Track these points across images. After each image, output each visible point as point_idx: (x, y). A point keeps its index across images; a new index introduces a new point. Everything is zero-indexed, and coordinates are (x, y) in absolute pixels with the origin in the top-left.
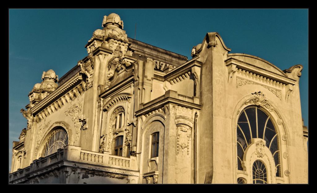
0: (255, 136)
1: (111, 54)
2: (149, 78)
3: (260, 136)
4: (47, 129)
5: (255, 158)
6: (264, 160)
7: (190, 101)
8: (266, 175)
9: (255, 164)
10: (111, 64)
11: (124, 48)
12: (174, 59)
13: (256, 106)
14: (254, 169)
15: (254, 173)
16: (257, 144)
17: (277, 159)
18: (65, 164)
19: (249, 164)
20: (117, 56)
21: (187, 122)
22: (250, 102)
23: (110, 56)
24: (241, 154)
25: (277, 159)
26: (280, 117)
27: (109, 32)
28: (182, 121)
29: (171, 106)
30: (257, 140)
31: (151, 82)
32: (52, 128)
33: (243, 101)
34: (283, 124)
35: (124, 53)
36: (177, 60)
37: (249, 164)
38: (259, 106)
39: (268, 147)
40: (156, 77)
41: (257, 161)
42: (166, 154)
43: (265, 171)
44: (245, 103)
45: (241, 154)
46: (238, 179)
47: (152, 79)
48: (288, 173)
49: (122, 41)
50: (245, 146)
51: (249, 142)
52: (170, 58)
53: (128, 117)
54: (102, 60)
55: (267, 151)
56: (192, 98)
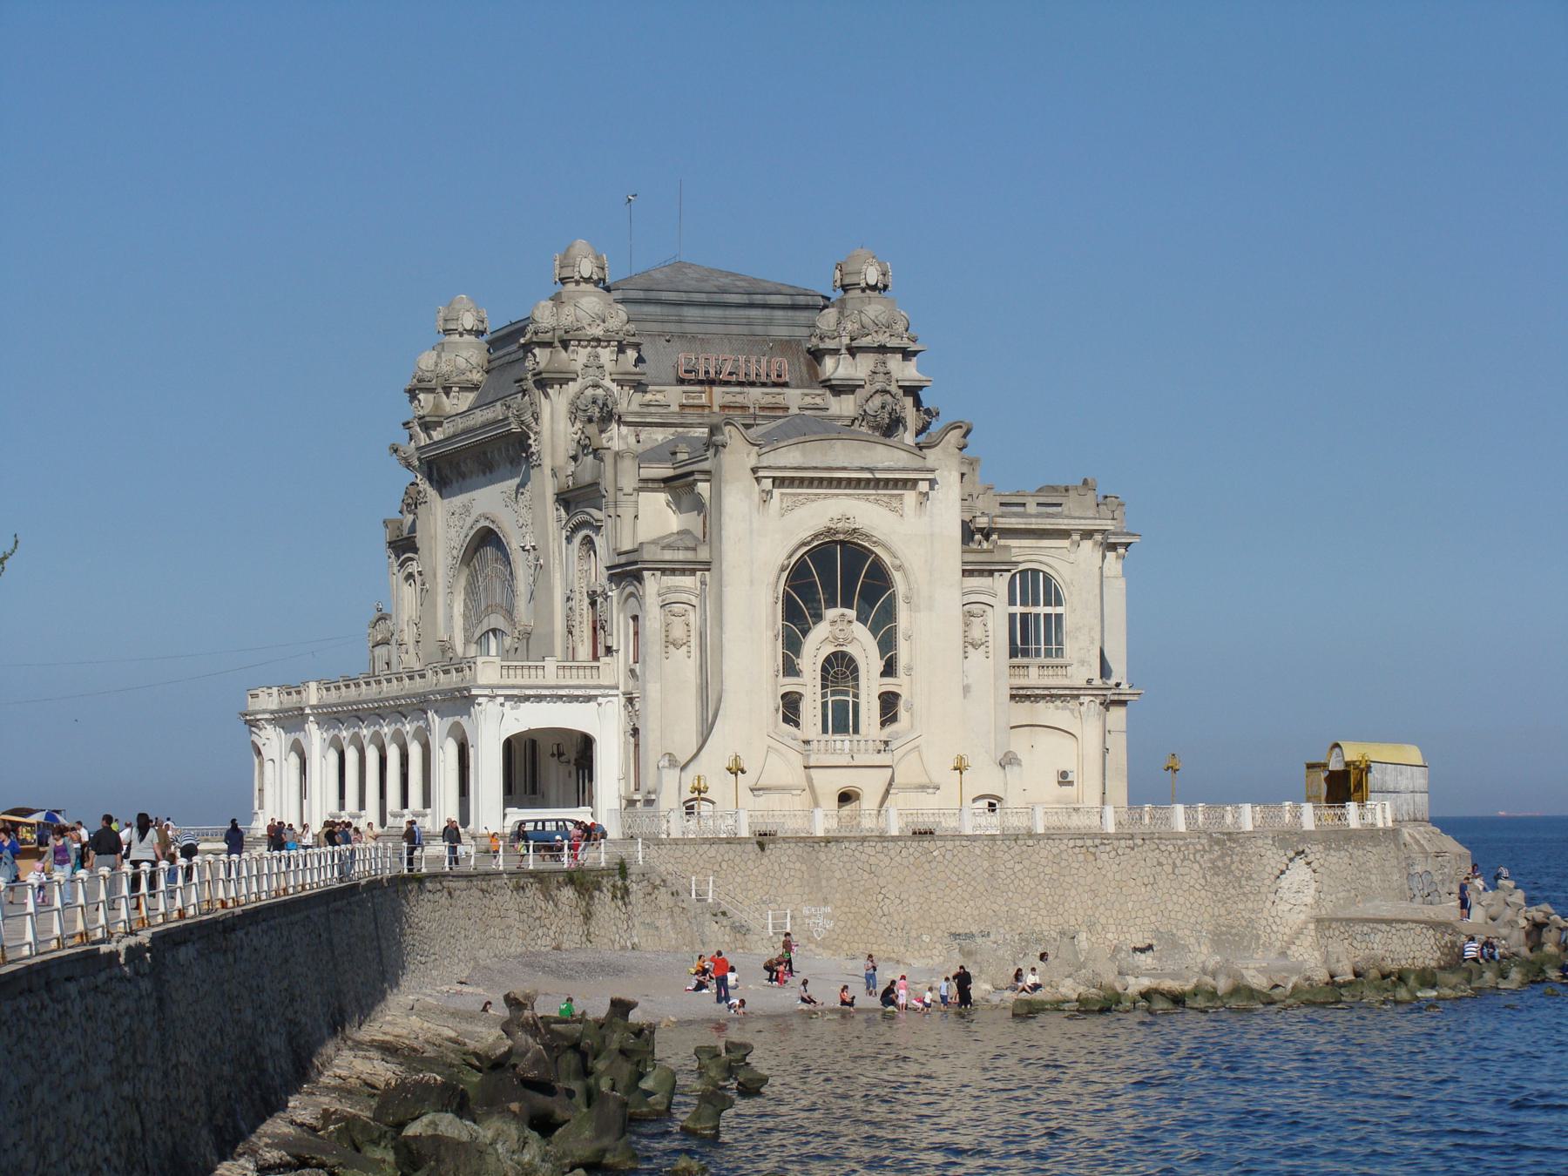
0: (831, 603)
1: (574, 380)
2: (628, 490)
3: (847, 604)
4: (469, 521)
5: (829, 649)
7: (690, 556)
8: (856, 679)
9: (828, 660)
10: (575, 412)
11: (606, 355)
12: (779, 313)
13: (836, 542)
14: (824, 669)
15: (824, 678)
16: (833, 622)
17: (887, 644)
18: (474, 692)
20: (589, 380)
21: (684, 597)
22: (816, 536)
23: (573, 388)
24: (792, 645)
25: (887, 644)
27: (567, 316)
28: (672, 597)
29: (646, 574)
30: (831, 614)
31: (632, 498)
32: (479, 526)
33: (795, 542)
35: (609, 366)
36: (790, 313)
38: (842, 543)
39: (864, 622)
40: (647, 484)
41: (835, 654)
42: (644, 661)
43: (856, 669)
44: (804, 544)
45: (792, 645)
46: (784, 696)
47: (639, 490)
49: (598, 340)
50: (805, 633)
51: (818, 617)
52: (767, 312)
55: (861, 632)
56: (694, 549)
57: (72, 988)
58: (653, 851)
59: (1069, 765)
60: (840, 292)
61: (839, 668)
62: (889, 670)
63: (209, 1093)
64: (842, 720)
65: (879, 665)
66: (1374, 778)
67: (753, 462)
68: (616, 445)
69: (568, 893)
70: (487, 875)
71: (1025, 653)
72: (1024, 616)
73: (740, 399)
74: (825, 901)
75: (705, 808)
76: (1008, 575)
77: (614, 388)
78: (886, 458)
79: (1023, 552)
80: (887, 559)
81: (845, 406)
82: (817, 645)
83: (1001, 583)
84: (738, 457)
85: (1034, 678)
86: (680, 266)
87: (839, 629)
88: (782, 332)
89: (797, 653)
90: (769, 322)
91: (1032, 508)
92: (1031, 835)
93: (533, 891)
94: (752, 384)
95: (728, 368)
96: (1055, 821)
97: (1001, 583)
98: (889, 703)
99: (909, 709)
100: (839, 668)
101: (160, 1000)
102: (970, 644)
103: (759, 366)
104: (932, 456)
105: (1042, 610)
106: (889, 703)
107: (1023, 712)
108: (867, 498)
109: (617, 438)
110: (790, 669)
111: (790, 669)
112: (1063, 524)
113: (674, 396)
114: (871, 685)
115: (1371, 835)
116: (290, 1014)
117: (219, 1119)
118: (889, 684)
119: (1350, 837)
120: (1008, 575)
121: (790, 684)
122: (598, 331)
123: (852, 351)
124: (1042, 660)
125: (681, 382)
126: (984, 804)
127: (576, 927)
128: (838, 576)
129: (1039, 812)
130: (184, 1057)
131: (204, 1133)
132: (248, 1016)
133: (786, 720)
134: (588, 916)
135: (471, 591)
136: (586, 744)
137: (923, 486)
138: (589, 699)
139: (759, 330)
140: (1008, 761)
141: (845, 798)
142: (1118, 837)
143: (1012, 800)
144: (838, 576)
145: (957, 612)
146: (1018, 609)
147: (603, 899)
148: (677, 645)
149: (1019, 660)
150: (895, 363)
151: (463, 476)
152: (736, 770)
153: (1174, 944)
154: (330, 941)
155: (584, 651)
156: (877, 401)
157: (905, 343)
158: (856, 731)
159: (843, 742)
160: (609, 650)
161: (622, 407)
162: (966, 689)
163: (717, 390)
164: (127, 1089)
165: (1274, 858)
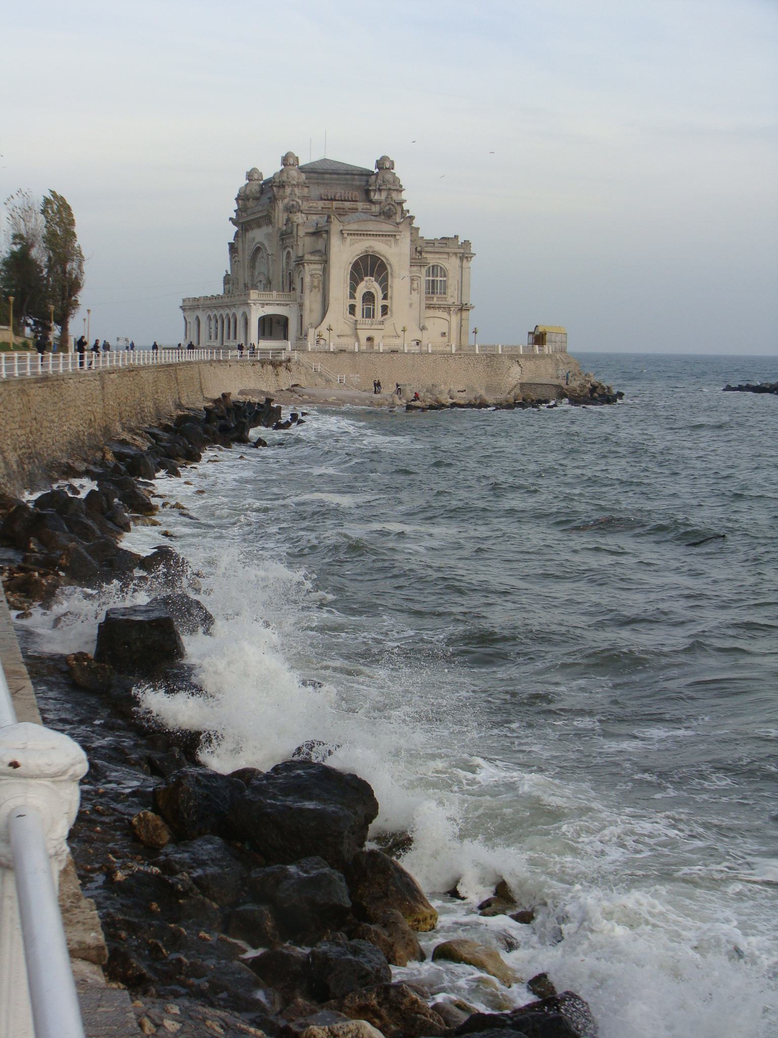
0: (366, 275)
5: (366, 290)
6: (372, 290)
17: (385, 289)
19: (359, 294)
21: (318, 272)
23: (286, 201)
24: (353, 289)
25: (385, 289)
26: (387, 260)
28: (314, 272)
30: (366, 278)
34: (390, 265)
35: (298, 194)
37: (359, 294)
45: (353, 289)
48: (391, 298)
53: (293, 264)
54: (281, 205)
55: (376, 285)
57: (71, 381)
58: (301, 355)
59: (445, 330)
60: (377, 170)
61: (369, 297)
62: (385, 297)
63: (120, 413)
64: (369, 314)
65: (381, 296)
66: (547, 337)
67: (341, 228)
68: (300, 221)
69: (270, 367)
70: (243, 361)
71: (433, 293)
72: (433, 281)
73: (341, 206)
74: (358, 373)
75: (322, 342)
76: (426, 268)
77: (300, 202)
78: (386, 227)
79: (432, 259)
80: (385, 261)
81: (376, 209)
82: (362, 289)
83: (424, 270)
84: (336, 227)
85: (435, 301)
86: (325, 160)
87: (369, 284)
88: (358, 183)
89: (355, 292)
90: (353, 180)
91: (436, 245)
92: (427, 353)
93: (259, 365)
94: (345, 201)
95: (338, 195)
96: (435, 349)
97: (424, 270)
98: (385, 309)
99: (391, 311)
100: (369, 297)
101: (103, 388)
102: (412, 289)
103: (349, 194)
104: (401, 227)
105: (439, 279)
106: (385, 309)
107: (431, 313)
108: (379, 241)
109: (299, 218)
110: (352, 296)
111: (352, 296)
112: (447, 250)
113: (321, 204)
114: (379, 302)
115: (542, 356)
116: (156, 396)
117: (124, 421)
118: (385, 302)
119: (535, 356)
120: (426, 268)
121: (352, 302)
122: (295, 183)
123: (380, 190)
124: (438, 295)
125: (322, 199)
126: (415, 343)
127: (273, 378)
128: (370, 266)
129: (430, 345)
130: (111, 403)
131: (118, 424)
132: (138, 395)
133: (350, 313)
134: (277, 375)
135: (253, 266)
136: (286, 319)
137: (398, 237)
138: (287, 305)
139: (350, 182)
140: (423, 329)
141: (370, 339)
142: (456, 355)
143: (424, 342)
144: (370, 266)
145: (408, 280)
146: (431, 278)
147: (282, 370)
148: (315, 287)
149: (431, 295)
150: (394, 195)
151: (252, 229)
152: (330, 329)
153: (473, 390)
154: (176, 379)
155: (287, 289)
156: (387, 208)
157: (398, 188)
158: (373, 317)
159: (369, 321)
160: (294, 289)
161: (302, 208)
162: (411, 305)
163: (334, 203)
164: (89, 408)
165: (508, 363)
